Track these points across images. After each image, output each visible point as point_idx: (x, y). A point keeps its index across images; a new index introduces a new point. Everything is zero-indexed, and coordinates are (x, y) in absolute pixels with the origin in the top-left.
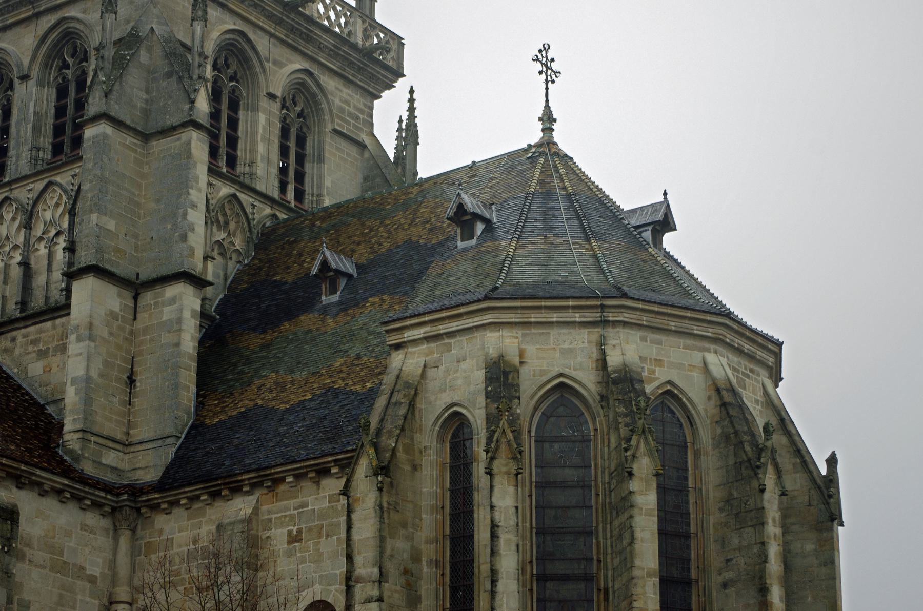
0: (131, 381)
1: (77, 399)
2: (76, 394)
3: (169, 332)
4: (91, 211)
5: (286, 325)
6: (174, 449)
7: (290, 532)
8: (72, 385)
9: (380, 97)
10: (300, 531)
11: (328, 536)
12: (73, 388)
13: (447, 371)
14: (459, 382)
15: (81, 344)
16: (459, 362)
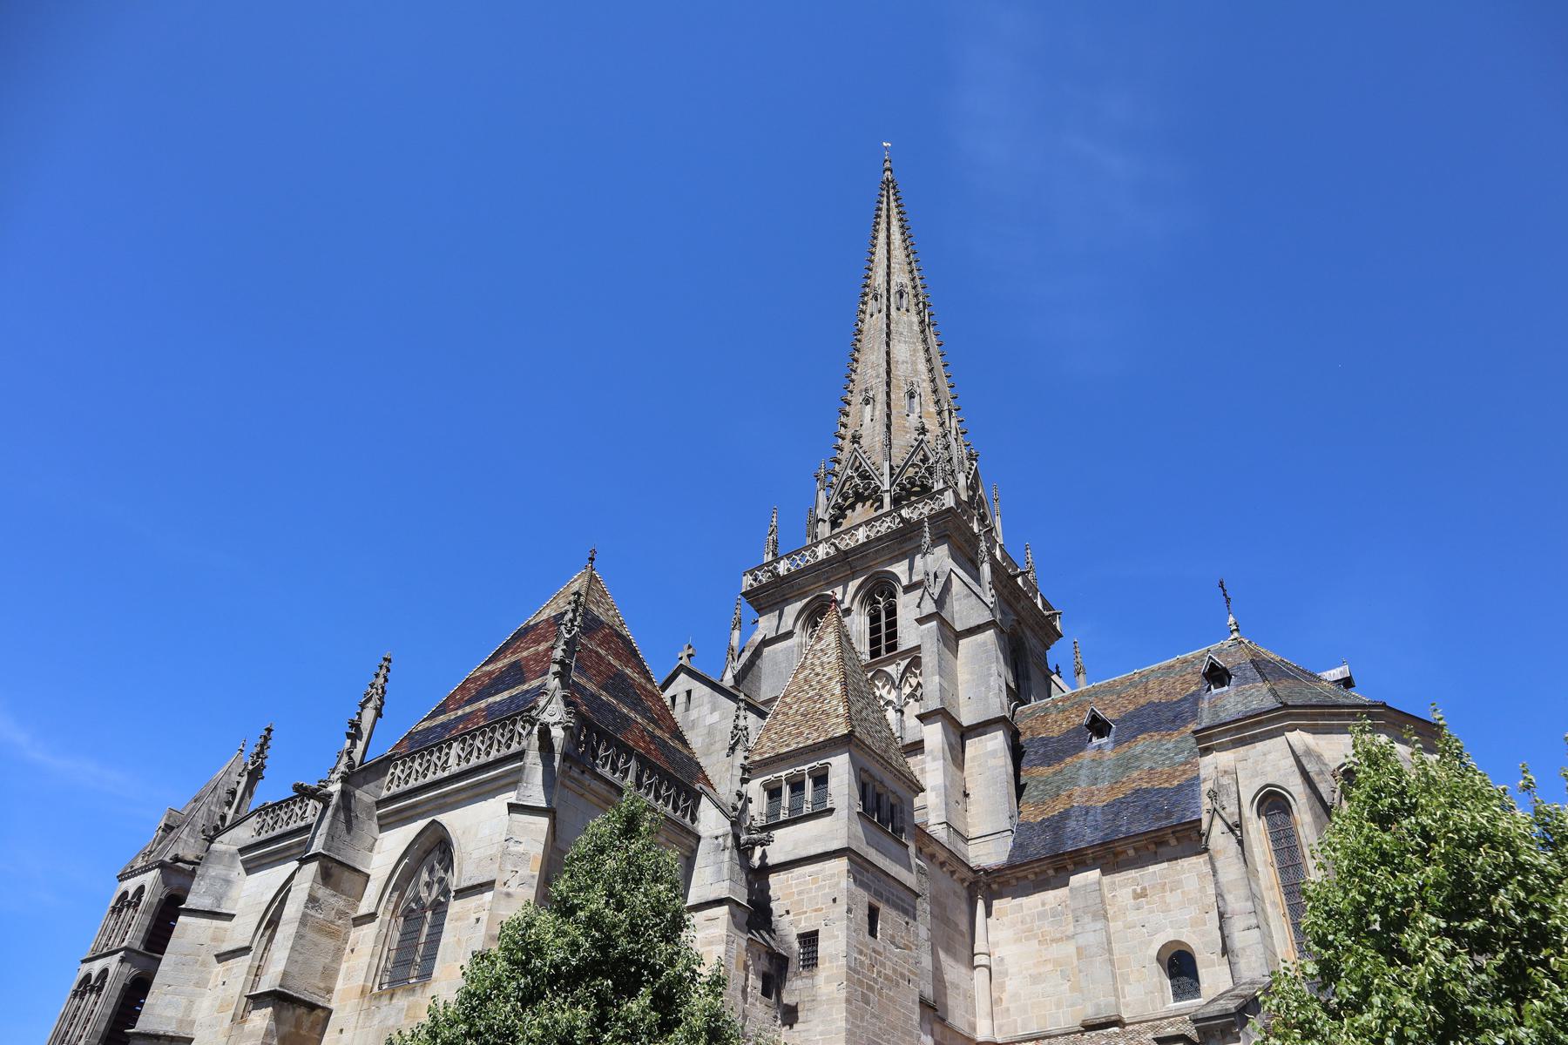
0: (966, 795)
1: (938, 800)
2: (937, 797)
3: (994, 758)
4: (933, 675)
5: (1068, 760)
6: (1012, 839)
7: (1134, 891)
8: (931, 791)
9: (1049, 648)
10: (1144, 889)
11: (1171, 891)
12: (934, 793)
13: (1256, 762)
14: (1269, 769)
15: (936, 763)
16: (1265, 755)
